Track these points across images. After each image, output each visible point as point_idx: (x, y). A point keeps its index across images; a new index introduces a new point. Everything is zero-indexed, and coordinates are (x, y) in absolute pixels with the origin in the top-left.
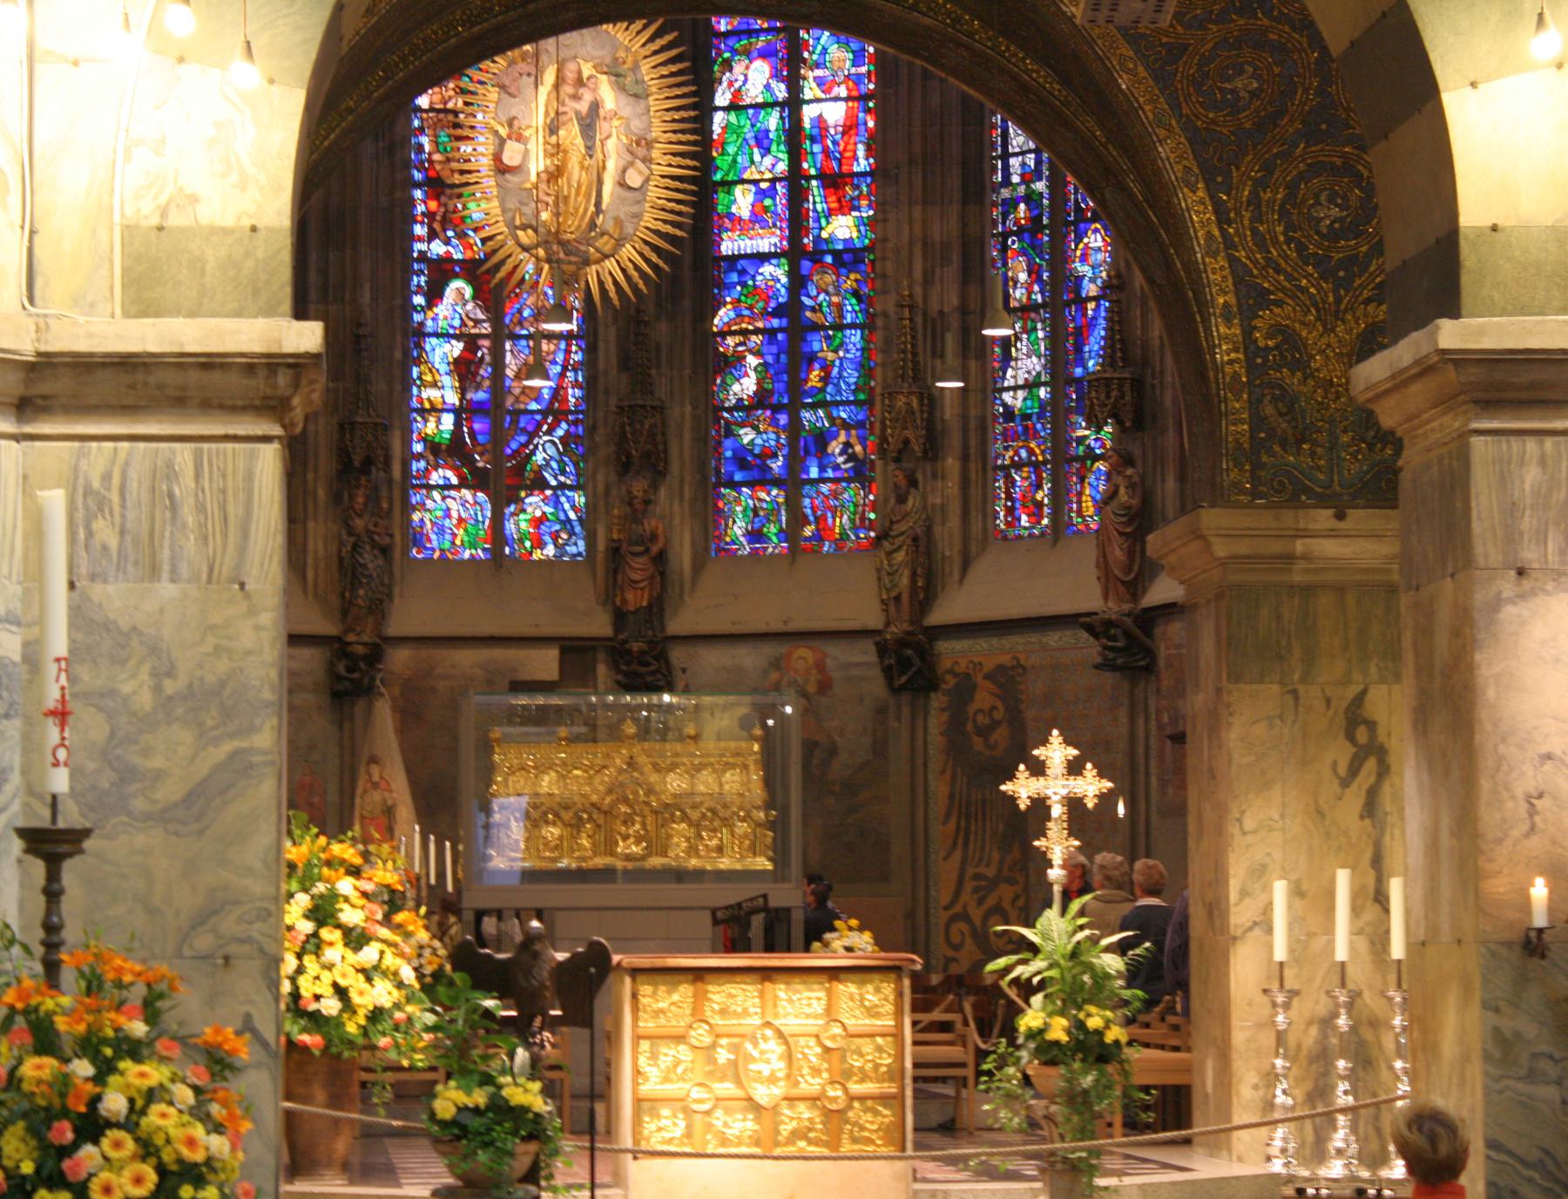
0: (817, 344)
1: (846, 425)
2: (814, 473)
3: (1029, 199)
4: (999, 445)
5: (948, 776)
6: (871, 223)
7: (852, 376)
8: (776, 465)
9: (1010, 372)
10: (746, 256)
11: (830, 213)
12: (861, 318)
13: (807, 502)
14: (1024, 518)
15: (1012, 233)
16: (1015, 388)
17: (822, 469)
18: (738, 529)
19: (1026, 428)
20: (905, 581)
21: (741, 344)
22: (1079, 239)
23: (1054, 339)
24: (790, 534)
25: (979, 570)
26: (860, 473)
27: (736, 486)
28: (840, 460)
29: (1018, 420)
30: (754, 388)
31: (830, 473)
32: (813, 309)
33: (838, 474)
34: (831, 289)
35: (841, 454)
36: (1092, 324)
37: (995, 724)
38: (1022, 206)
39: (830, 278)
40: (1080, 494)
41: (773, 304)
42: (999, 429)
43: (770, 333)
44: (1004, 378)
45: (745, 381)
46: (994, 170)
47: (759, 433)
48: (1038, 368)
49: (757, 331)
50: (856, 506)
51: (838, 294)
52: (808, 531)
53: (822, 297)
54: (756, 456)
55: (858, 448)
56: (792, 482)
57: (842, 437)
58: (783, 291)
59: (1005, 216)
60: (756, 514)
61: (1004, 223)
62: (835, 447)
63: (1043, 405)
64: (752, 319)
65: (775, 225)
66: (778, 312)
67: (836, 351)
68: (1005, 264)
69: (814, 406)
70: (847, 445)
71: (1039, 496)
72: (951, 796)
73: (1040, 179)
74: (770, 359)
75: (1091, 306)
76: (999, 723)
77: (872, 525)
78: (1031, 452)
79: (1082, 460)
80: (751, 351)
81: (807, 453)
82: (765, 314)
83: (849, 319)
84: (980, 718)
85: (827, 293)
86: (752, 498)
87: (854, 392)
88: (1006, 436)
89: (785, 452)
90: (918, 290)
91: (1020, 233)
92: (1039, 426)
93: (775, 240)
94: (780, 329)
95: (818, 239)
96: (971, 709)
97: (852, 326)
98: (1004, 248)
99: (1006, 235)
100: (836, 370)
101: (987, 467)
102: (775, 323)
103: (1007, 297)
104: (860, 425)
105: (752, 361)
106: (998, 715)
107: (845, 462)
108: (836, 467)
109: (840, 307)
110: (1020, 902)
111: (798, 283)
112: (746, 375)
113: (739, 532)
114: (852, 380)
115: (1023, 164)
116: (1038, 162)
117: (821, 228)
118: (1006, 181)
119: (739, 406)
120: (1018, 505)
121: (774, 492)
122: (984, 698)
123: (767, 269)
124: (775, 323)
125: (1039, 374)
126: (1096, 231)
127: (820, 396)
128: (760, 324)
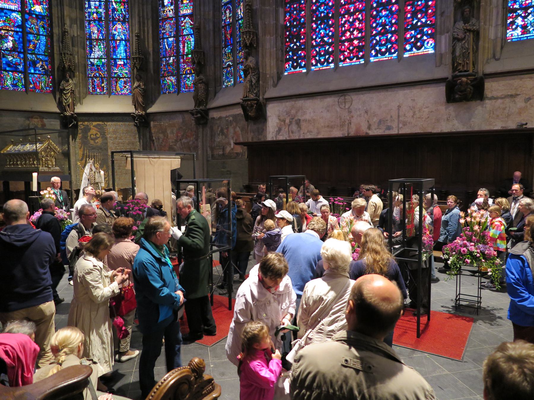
0: (31, 37)
1: (41, 60)
2: (32, 71)
3: (97, 13)
4: (89, 72)
5: (82, 149)
6: (47, 9)
7: (43, 48)
8: (20, 67)
9: (92, 54)
10: (6, 9)
11: (34, 4)
12: (45, 34)
13: (31, 78)
14: (98, 90)
15: (92, 20)
16: (94, 58)
17: (35, 70)
18: (9, 83)
19: (98, 69)
20: (70, 101)
21: (6, 33)
22: (114, 25)
23: (107, 47)
24: (25, 86)
25: (85, 101)
26: (46, 73)
27: (8, 71)
28: (40, 69)
29: (95, 66)
30: (11, 46)
31: (37, 72)
32: (30, 28)
33: (40, 73)
34: (35, 24)
35: (40, 67)
36: (119, 46)
37: (97, 138)
38: (95, 14)
39: (35, 21)
40: (116, 86)
41: (17, 24)
42: (89, 68)
43: (17, 32)
44: (90, 55)
45: (9, 43)
46: (86, 4)
47: (14, 58)
48: (101, 54)
49: (12, 31)
50: (46, 81)
51: (38, 26)
52: (31, 86)
53: (32, 26)
54: (14, 64)
55: (46, 67)
56: (25, 73)
57: (41, 63)
58: (20, 21)
59: (89, 16)
60: (14, 79)
61: (89, 17)
62: (39, 65)
63: (103, 64)
64: (10, 27)
65: (16, 3)
66: (18, 26)
67: (38, 40)
68: (90, 28)
69: (32, 54)
70: (42, 66)
71: (103, 85)
72: (83, 155)
73: (101, 8)
74: (17, 39)
75: (118, 42)
76: (99, 137)
77: (51, 86)
78: (100, 74)
79: (116, 78)
80: (10, 36)
81: (30, 66)
82: (14, 26)
83: (41, 33)
84: (92, 136)
85: (34, 25)
86: (12, 75)
87: (44, 52)
88: (91, 70)
89: (23, 64)
90: (68, 29)
91: (94, 21)
92: (102, 68)
93: (16, 7)
94: (19, 32)
95: (30, 10)
96: (89, 134)
97: (42, 35)
98: (89, 24)
99: (89, 21)
100: (38, 46)
101: (86, 77)
102: (18, 29)
103: (90, 35)
104: (46, 61)
105: (10, 38)
106: (98, 136)
107: (42, 70)
108: (39, 71)
109: (38, 30)
110: (107, 179)
111: (24, 20)
112: (9, 42)
113: (9, 84)
114: (43, 49)
115: (95, 4)
116: (100, 5)
117: (31, 7)
118: (90, 7)
119: (7, 49)
120: (96, 86)
121: (20, 74)
122: (93, 131)
123: (14, 14)
124: (18, 29)
125: (102, 56)
126: (119, 24)
127: (33, 52)
128: (13, 29)
